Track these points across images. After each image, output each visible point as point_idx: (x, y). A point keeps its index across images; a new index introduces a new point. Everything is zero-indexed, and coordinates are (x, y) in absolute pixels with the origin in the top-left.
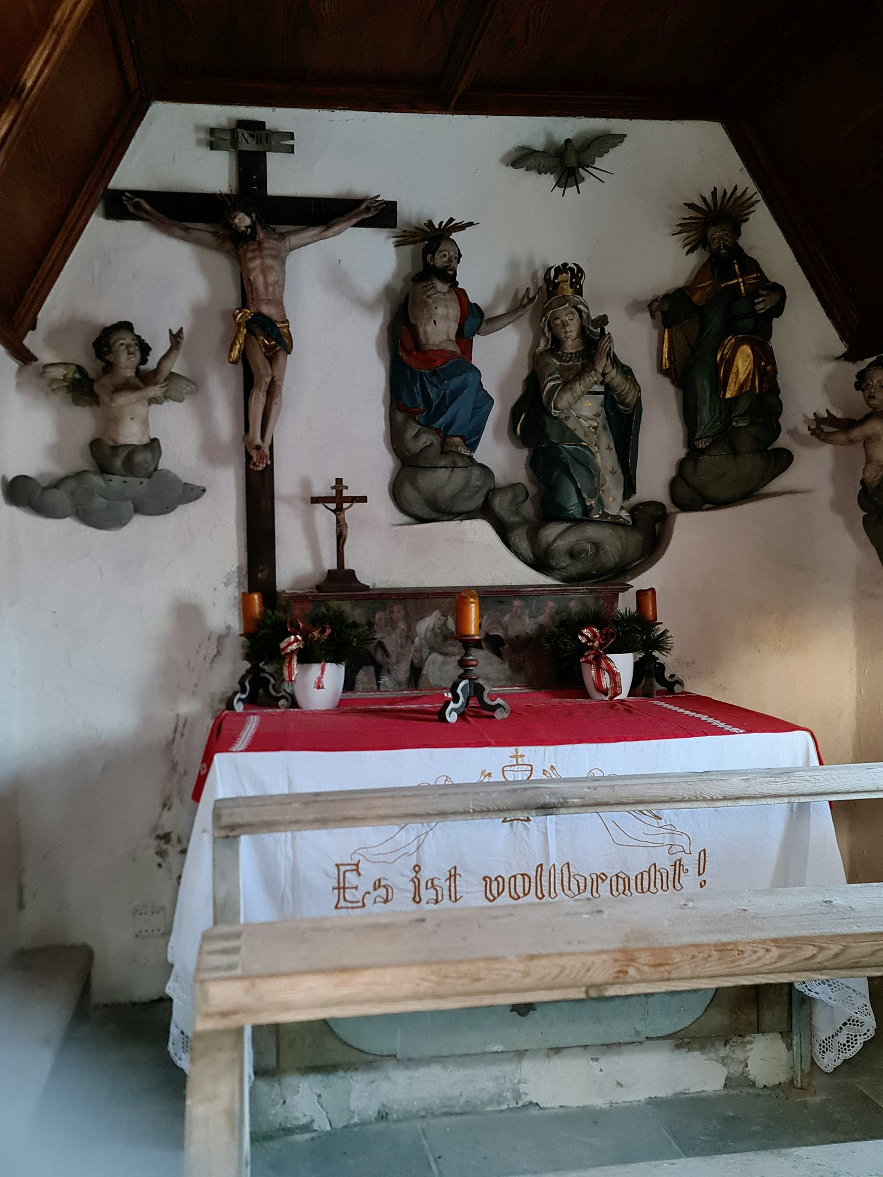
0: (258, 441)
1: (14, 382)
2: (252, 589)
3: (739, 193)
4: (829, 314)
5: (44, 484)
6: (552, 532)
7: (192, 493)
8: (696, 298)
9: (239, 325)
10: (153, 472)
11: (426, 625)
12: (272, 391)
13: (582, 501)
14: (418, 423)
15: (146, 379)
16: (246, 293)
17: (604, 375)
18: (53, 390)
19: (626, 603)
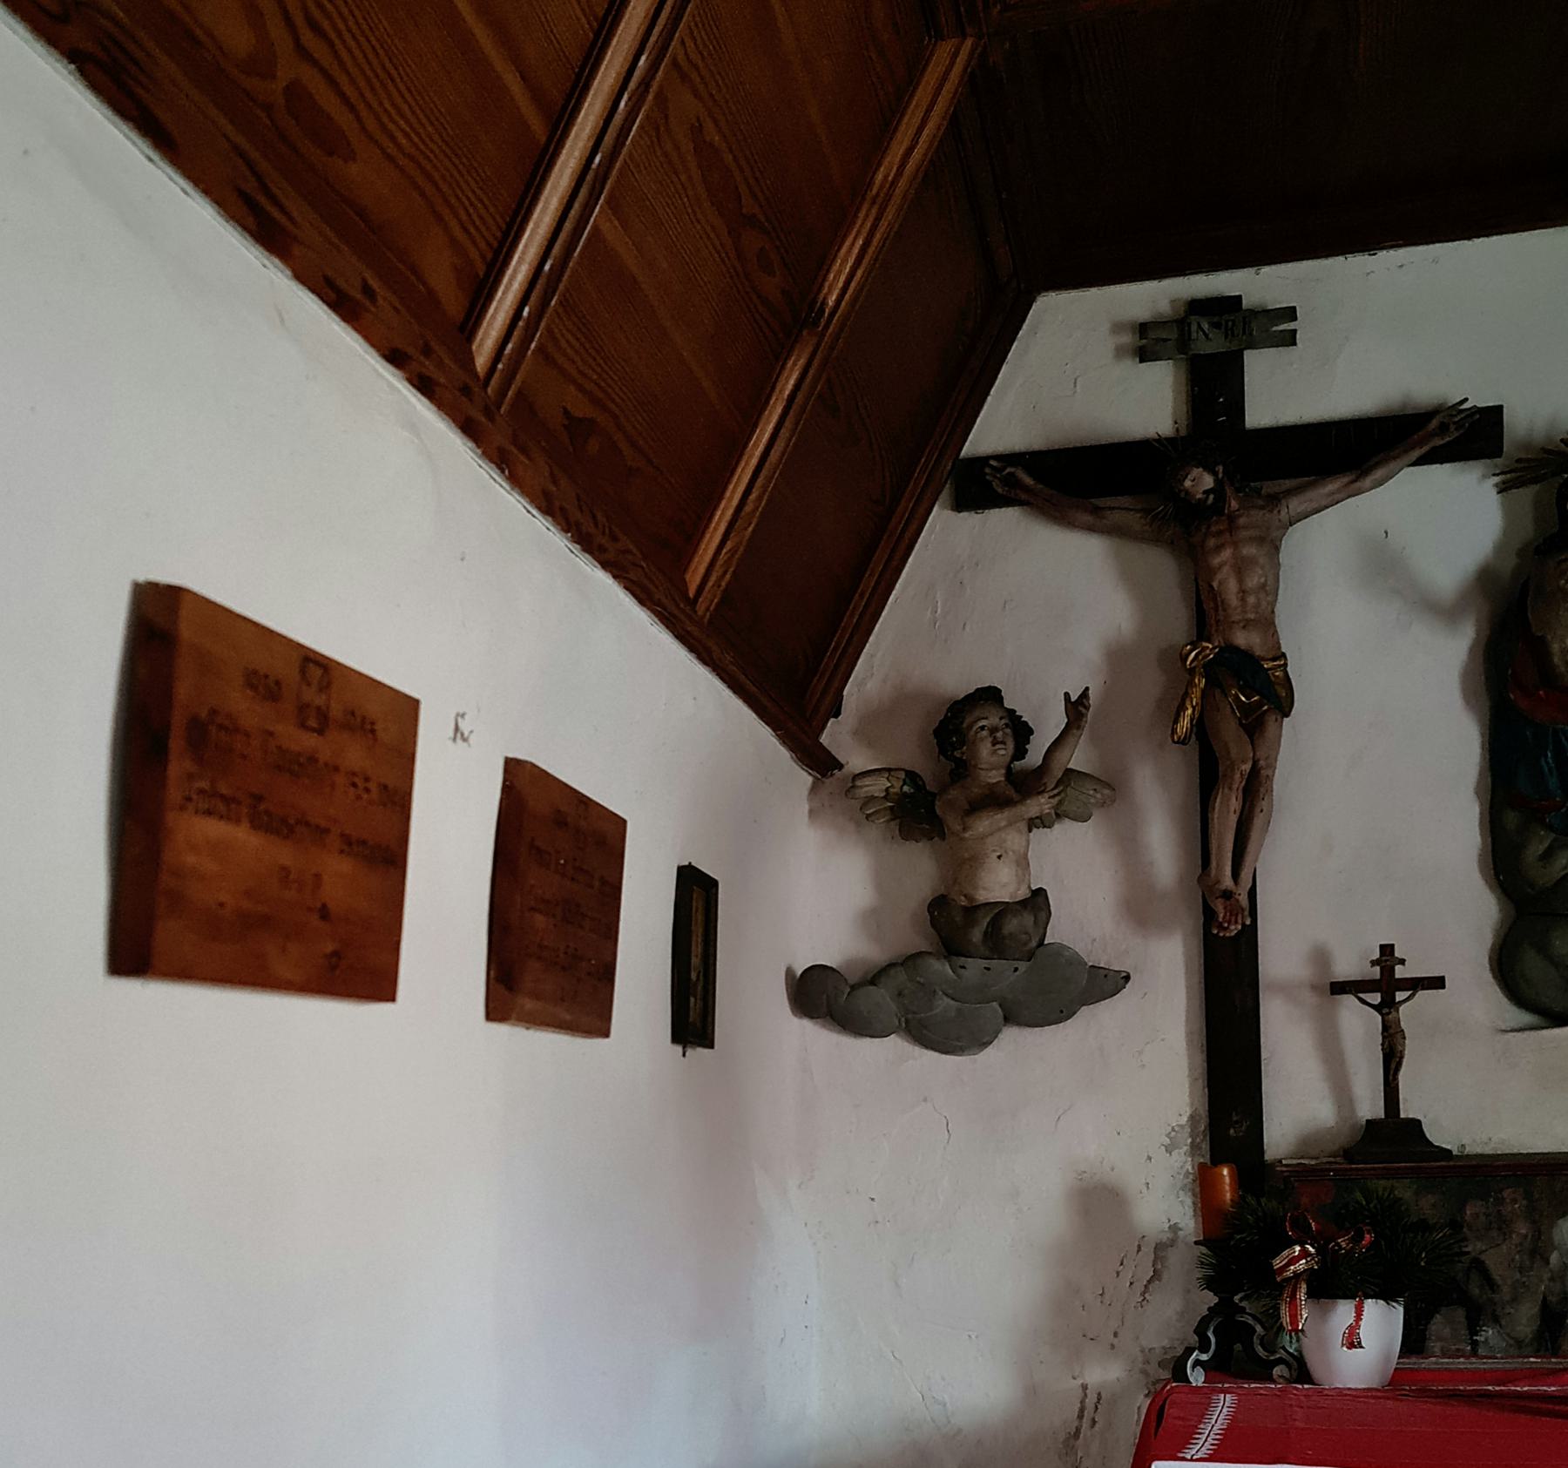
0: (1228, 882)
1: (806, 807)
2: (1217, 1158)
5: (852, 980)
7: (1105, 983)
9: (1192, 672)
10: (1035, 950)
12: (1255, 788)
14: (1550, 828)
15: (1024, 784)
16: (1206, 612)
18: (868, 816)
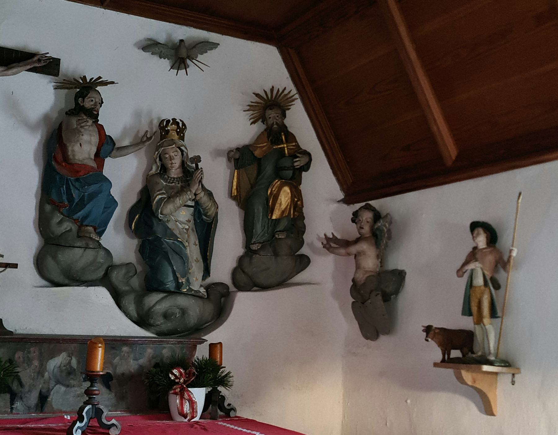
3: (286, 92)
4: (335, 173)
6: (153, 298)
8: (257, 153)
11: (55, 363)
13: (176, 279)
14: (62, 214)
17: (195, 195)
19: (202, 352)
